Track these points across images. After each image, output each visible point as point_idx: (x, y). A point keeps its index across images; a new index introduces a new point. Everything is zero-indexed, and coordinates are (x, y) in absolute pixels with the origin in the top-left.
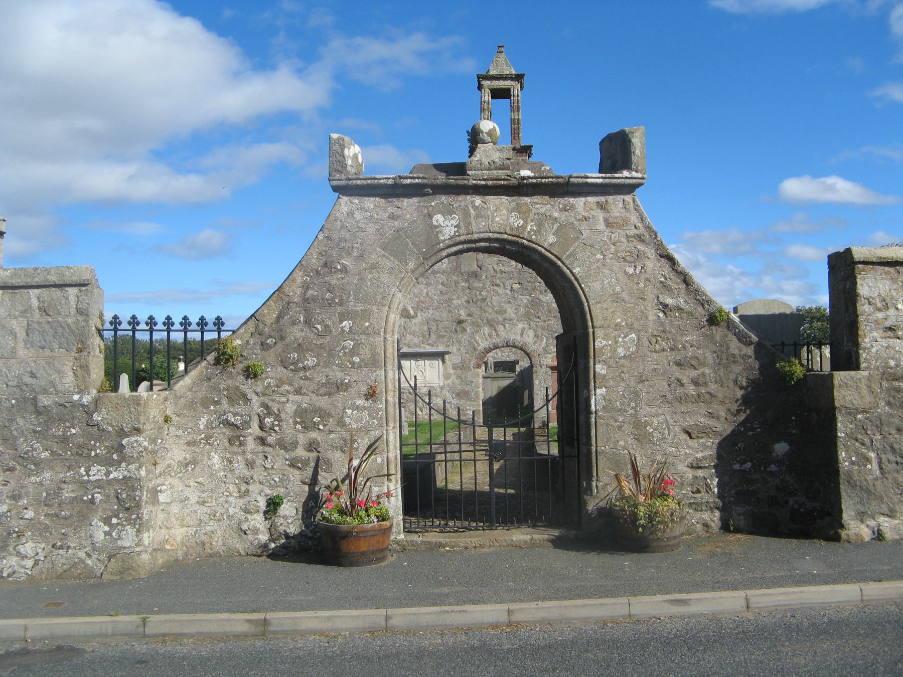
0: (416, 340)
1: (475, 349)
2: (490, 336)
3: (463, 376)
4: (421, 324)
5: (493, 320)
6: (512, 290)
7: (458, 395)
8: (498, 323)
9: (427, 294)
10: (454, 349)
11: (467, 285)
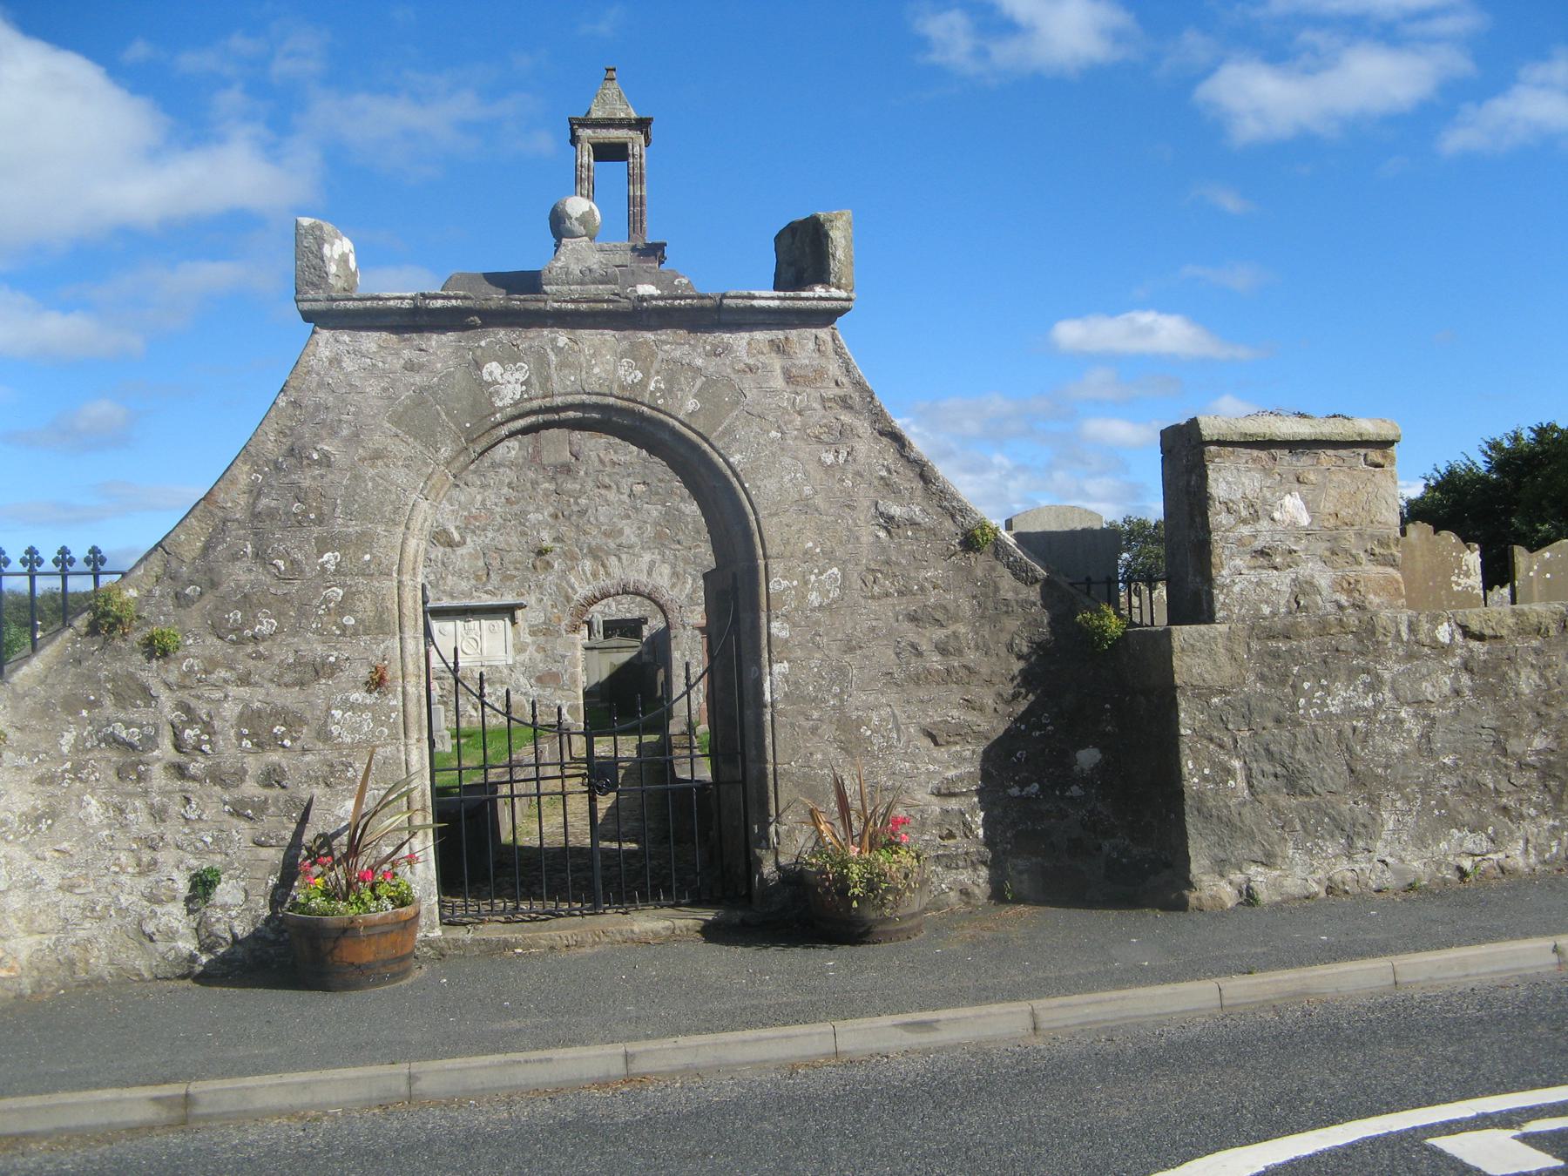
0: (465, 585)
1: (568, 599)
2: (595, 575)
5: (599, 548)
6: (631, 495)
7: (540, 679)
8: (608, 554)
9: (483, 502)
10: (531, 600)
11: (552, 487)
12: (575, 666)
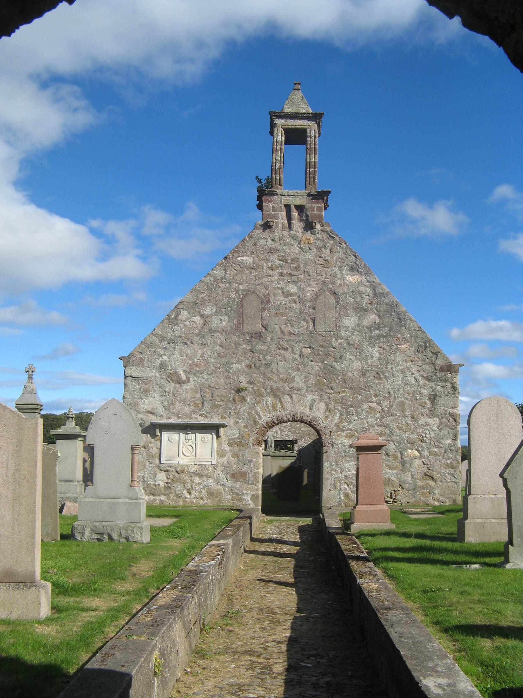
0: (187, 410)
1: (255, 422)
2: (274, 407)
3: (240, 454)
4: (194, 391)
5: (278, 389)
6: (301, 355)
7: (233, 476)
8: (284, 393)
9: (202, 355)
10: (230, 422)
11: (249, 347)
12: (258, 468)
